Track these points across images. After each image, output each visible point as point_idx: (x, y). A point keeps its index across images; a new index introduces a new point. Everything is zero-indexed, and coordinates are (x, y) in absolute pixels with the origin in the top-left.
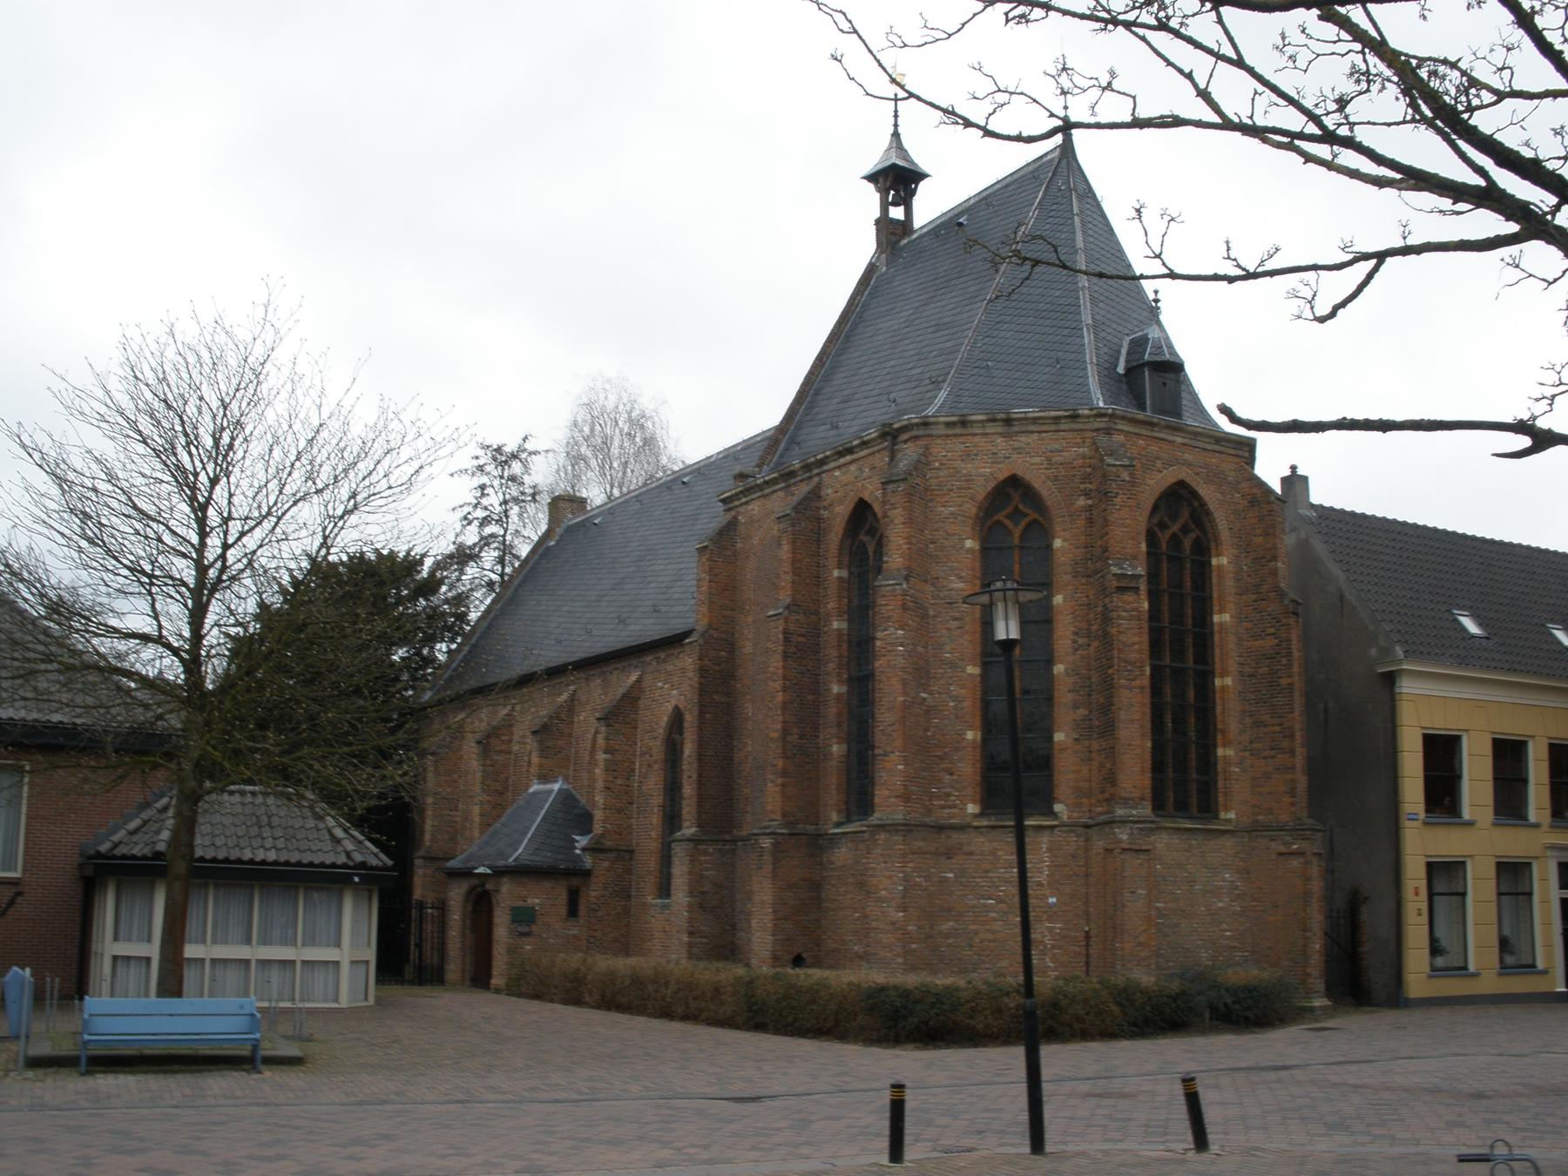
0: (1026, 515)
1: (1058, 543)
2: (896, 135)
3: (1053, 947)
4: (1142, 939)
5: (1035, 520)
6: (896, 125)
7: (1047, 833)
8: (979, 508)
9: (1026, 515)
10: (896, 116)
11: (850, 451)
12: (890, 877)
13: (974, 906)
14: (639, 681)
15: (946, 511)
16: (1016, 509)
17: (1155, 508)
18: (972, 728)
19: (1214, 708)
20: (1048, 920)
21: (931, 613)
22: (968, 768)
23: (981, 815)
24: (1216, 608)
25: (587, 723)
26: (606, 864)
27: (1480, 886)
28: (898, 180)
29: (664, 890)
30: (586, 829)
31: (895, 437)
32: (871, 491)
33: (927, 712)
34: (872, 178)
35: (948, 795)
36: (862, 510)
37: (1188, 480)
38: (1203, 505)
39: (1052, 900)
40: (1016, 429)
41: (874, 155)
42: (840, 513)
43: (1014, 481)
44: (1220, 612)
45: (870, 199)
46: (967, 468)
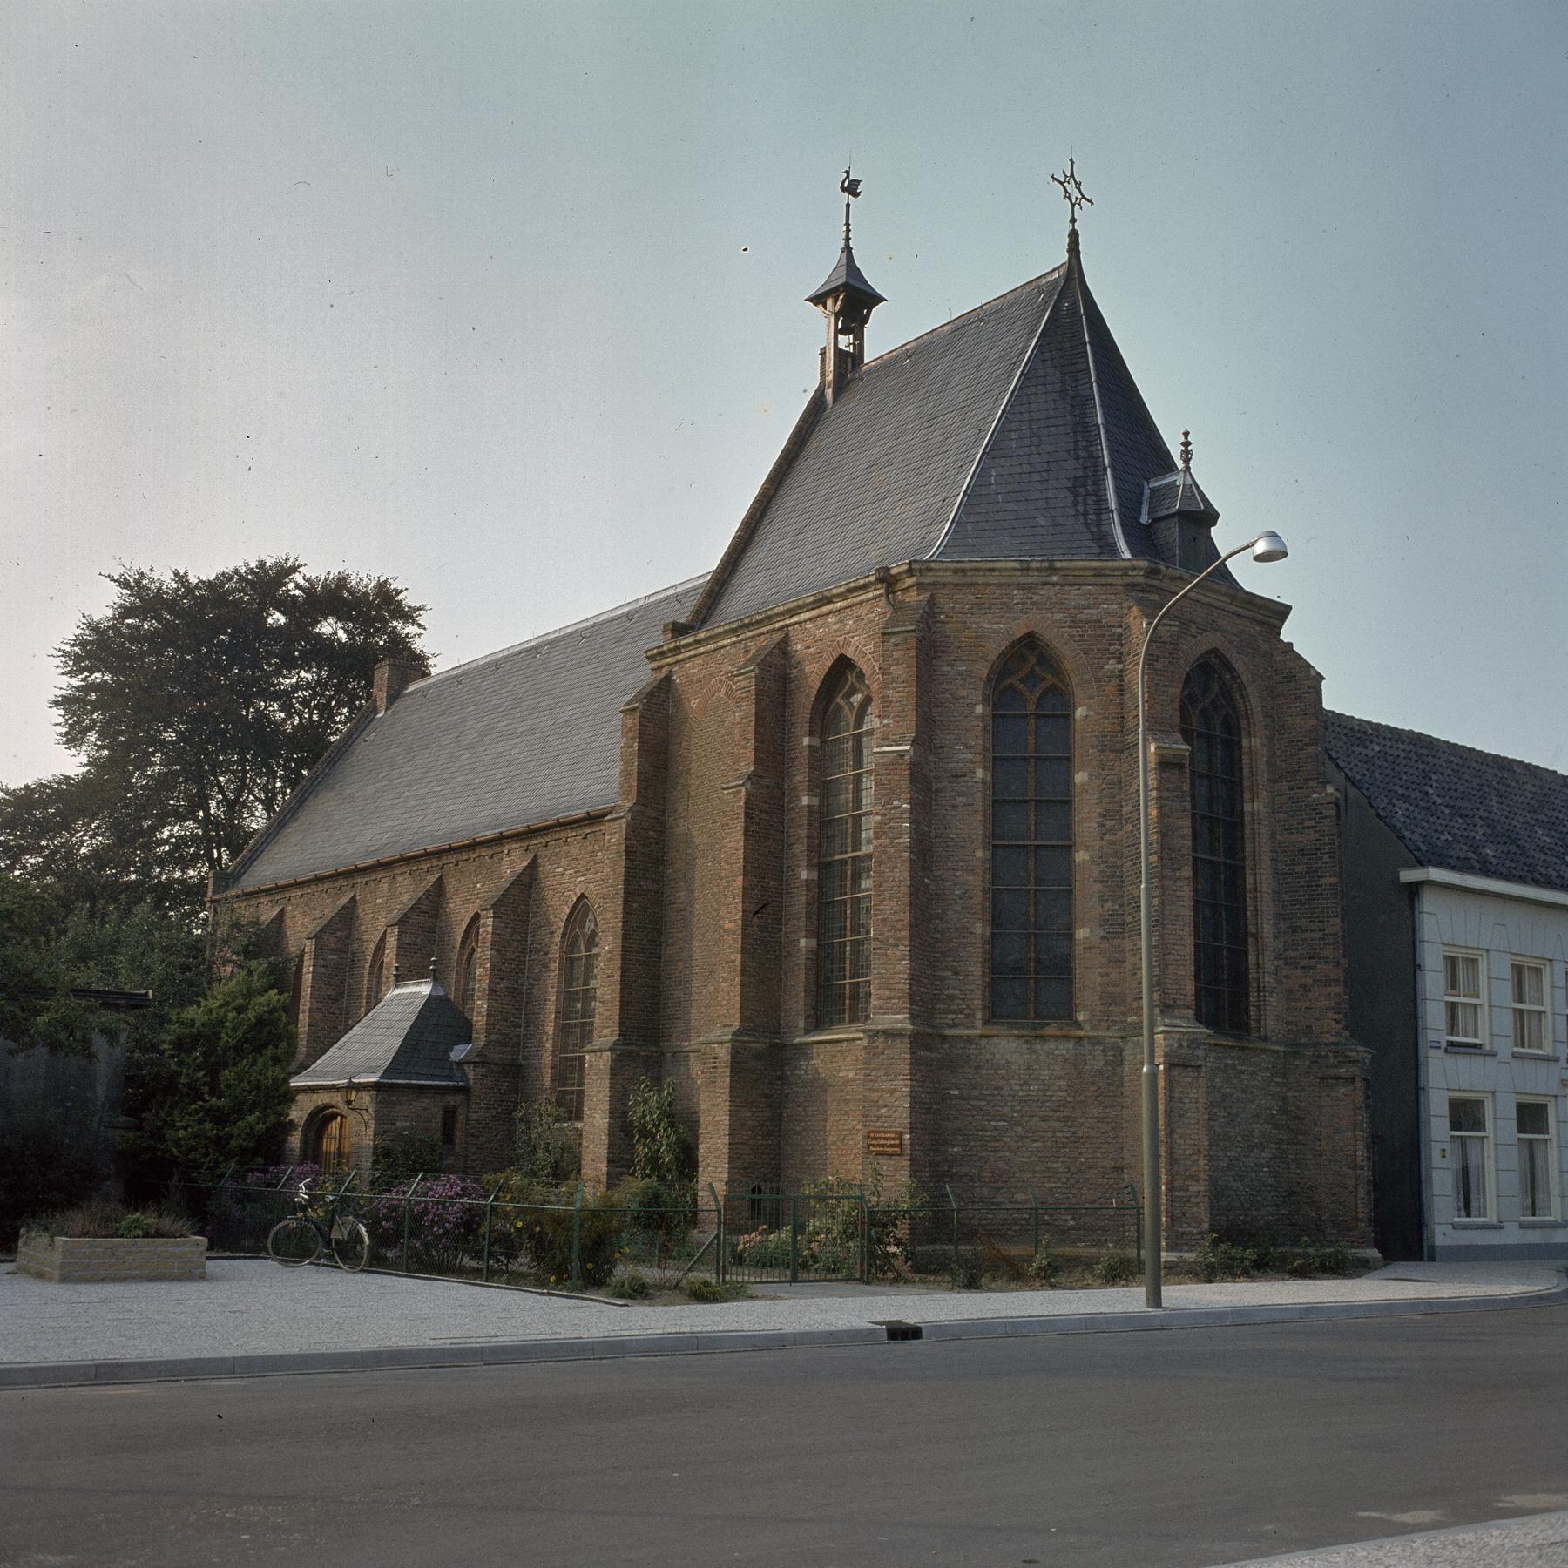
1: (1080, 713)
2: (848, 250)
5: (1053, 688)
6: (848, 239)
10: (848, 230)
11: (829, 601)
17: (1188, 679)
19: (1245, 910)
27: (1500, 1126)
28: (852, 300)
30: (467, 1039)
32: (862, 648)
34: (818, 299)
35: (953, 997)
36: (843, 666)
38: (1236, 677)
41: (823, 270)
42: (814, 671)
43: (1030, 642)
45: (819, 326)
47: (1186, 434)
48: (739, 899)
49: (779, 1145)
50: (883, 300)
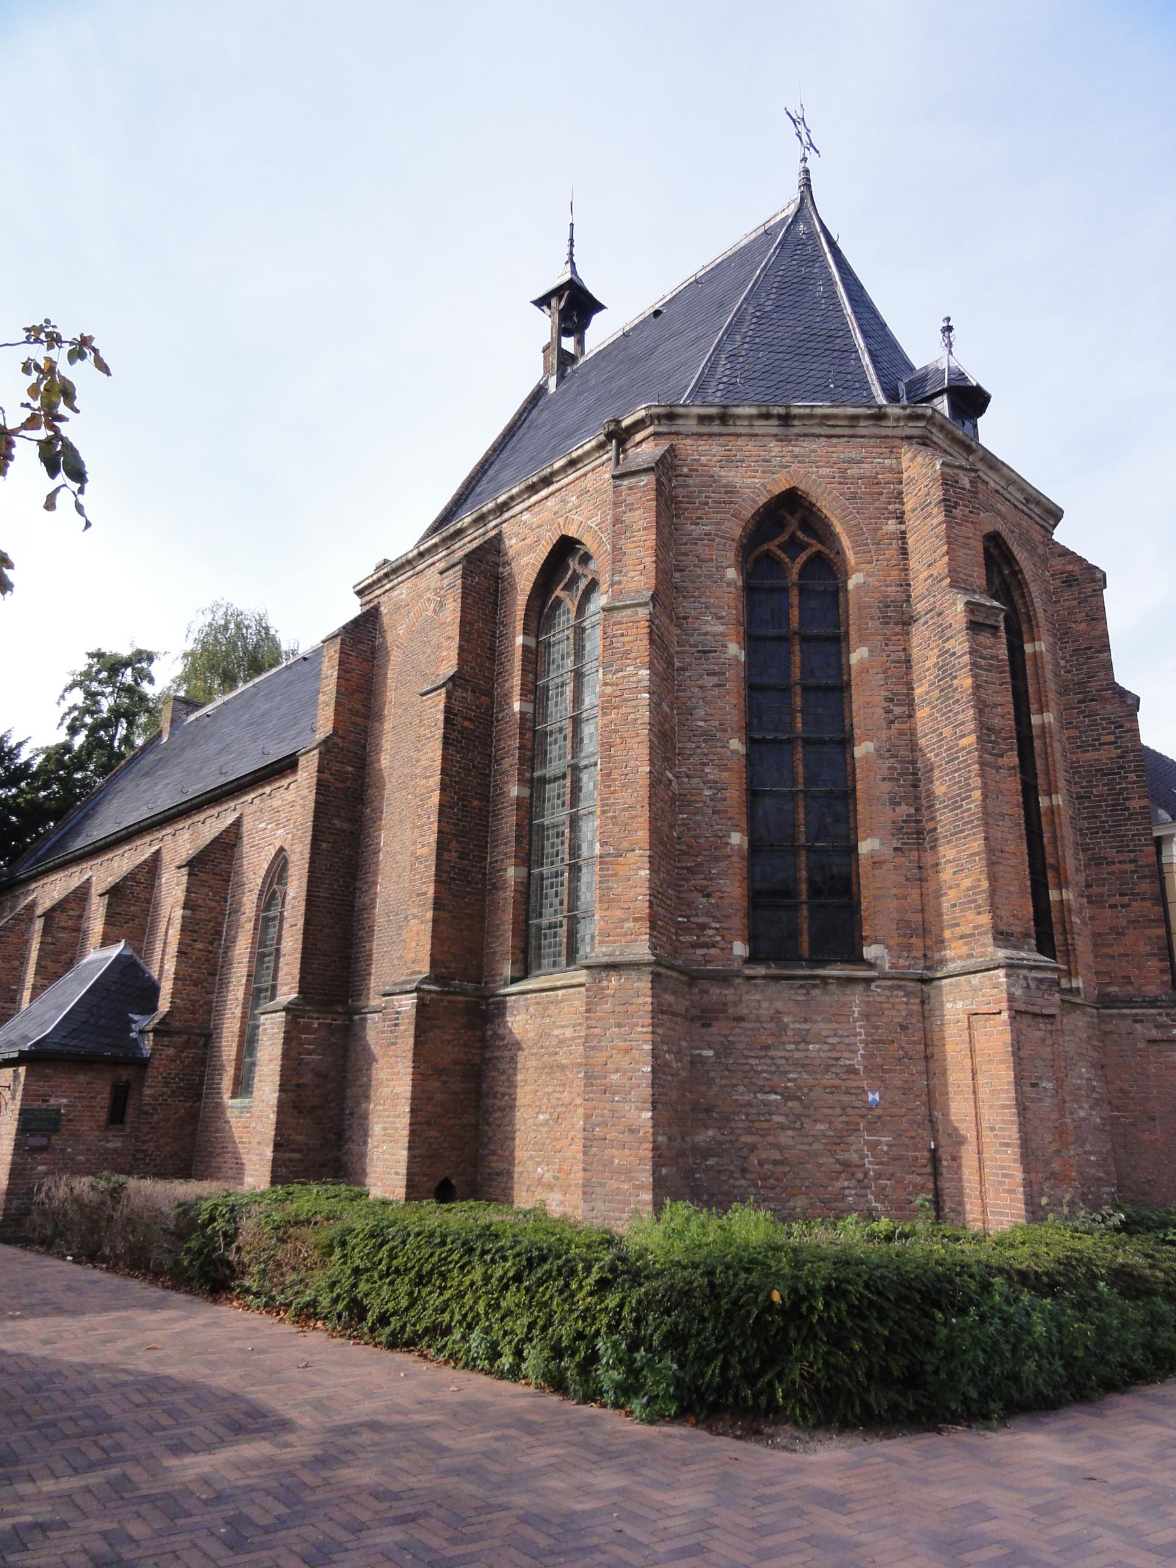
0: (804, 547)
3: (879, 1175)
4: (1055, 1166)
6: (571, 254)
7: (860, 988)
8: (744, 528)
9: (809, 545)
10: (572, 245)
12: (628, 1051)
13: (749, 1104)
14: (238, 823)
15: (698, 530)
16: (793, 537)
18: (736, 828)
19: (1042, 837)
20: (870, 1134)
21: (677, 664)
22: (732, 888)
23: (752, 959)
24: (1034, 707)
25: (173, 890)
26: (171, 1051)
28: (574, 305)
29: (243, 1086)
31: (621, 443)
33: (673, 800)
34: (542, 302)
35: (703, 927)
36: (566, 548)
37: (1003, 534)
39: (874, 1097)
40: (796, 430)
44: (1041, 711)
45: (544, 324)
46: (731, 476)
47: (948, 319)
48: (434, 818)
49: (476, 1127)
50: (599, 307)
